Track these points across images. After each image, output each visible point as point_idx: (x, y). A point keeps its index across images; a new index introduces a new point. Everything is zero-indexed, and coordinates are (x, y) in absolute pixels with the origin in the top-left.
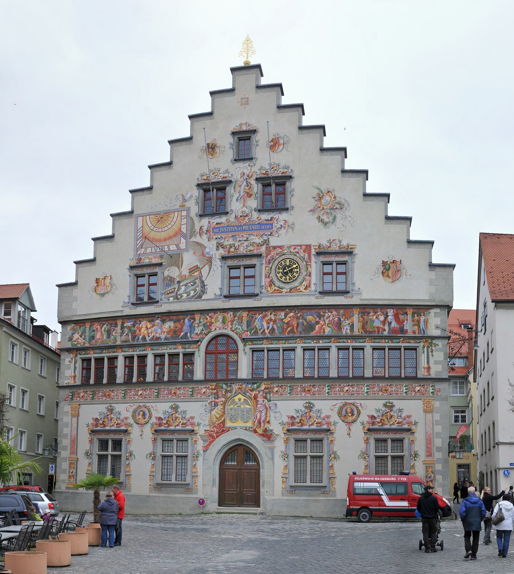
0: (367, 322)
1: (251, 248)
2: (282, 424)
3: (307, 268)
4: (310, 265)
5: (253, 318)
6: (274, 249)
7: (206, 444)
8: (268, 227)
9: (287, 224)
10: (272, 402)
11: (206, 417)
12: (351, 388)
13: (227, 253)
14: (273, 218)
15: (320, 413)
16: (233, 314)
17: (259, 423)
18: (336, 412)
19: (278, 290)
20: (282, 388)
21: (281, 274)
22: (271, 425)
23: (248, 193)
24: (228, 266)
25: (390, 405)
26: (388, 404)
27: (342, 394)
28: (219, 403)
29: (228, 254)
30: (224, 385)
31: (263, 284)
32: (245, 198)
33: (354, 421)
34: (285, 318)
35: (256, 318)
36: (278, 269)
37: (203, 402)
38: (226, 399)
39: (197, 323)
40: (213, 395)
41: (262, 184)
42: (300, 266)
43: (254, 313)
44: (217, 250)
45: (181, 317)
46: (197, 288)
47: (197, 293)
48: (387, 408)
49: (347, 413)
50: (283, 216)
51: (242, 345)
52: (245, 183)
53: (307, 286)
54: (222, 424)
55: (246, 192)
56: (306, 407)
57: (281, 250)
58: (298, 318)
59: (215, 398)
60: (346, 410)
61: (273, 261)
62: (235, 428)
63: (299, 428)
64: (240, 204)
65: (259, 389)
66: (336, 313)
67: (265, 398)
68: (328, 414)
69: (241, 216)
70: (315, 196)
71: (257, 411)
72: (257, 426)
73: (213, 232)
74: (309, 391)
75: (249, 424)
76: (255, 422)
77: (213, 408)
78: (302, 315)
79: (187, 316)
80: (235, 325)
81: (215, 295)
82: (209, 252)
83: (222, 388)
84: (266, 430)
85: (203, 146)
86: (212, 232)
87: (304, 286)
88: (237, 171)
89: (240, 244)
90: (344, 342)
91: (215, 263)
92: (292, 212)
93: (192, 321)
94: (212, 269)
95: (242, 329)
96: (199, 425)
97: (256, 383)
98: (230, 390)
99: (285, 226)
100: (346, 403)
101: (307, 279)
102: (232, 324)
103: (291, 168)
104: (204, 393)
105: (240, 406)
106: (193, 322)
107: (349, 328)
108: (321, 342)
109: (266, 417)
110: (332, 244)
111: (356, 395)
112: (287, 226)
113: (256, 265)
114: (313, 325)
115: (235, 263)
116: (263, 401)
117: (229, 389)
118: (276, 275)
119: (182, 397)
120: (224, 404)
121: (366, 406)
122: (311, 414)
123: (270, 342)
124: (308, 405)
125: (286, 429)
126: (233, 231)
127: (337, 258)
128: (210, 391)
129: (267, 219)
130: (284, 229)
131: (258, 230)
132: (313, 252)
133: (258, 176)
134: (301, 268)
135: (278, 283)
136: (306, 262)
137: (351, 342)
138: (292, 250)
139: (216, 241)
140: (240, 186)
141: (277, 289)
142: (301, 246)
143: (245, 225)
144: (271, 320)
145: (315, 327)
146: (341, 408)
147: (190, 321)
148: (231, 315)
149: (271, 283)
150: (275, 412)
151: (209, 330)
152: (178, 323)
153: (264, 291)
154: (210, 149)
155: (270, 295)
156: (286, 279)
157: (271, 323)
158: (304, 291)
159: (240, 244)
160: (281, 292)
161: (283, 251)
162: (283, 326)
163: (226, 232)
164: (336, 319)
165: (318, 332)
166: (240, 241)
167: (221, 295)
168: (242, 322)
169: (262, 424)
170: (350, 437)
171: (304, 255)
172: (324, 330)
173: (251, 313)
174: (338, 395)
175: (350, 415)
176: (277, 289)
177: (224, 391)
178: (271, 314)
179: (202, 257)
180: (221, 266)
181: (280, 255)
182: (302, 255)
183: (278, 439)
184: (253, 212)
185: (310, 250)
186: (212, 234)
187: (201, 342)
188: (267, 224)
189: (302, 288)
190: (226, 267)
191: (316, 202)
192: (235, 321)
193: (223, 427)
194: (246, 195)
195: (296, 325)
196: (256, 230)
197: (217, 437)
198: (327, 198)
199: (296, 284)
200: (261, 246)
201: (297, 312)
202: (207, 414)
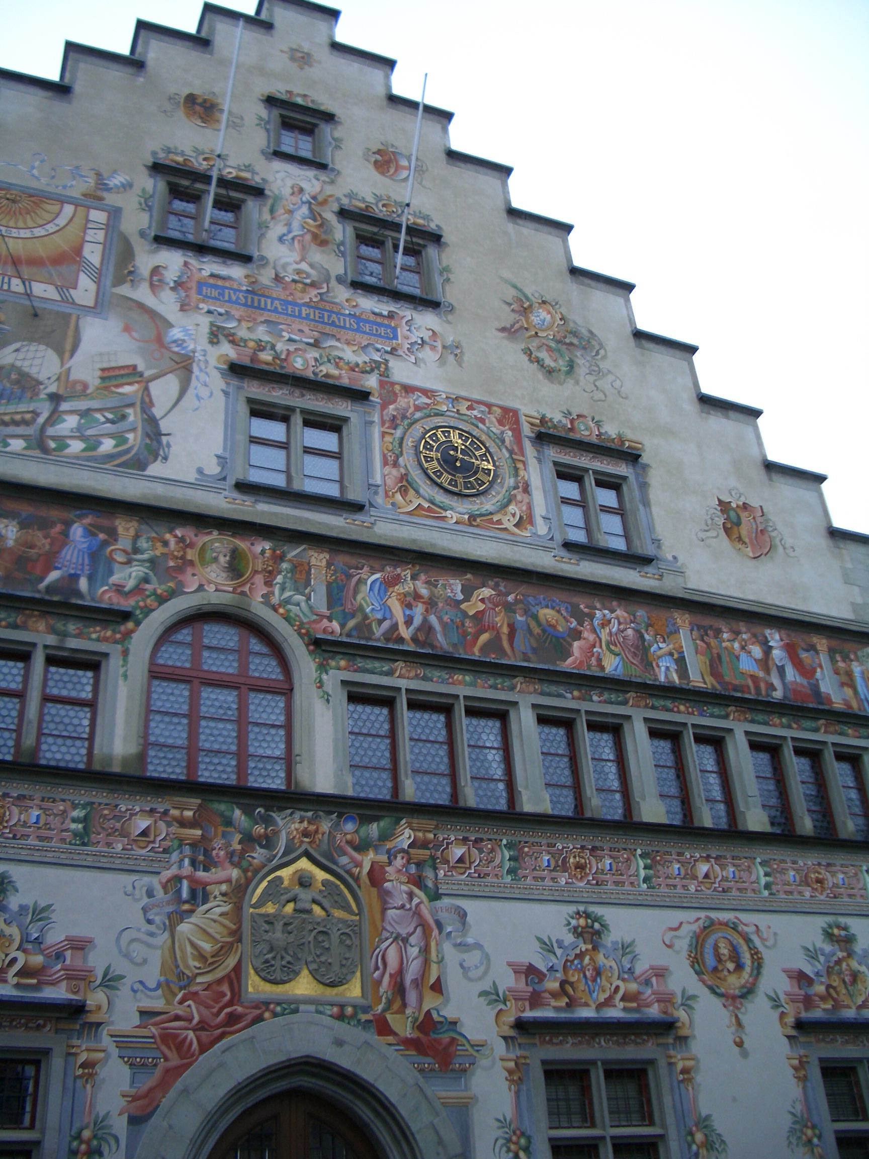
0: (719, 657)
2: (493, 996)
3: (516, 469)
4: (524, 463)
5: (350, 577)
7: (149, 1081)
8: (382, 331)
9: (438, 340)
10: (446, 901)
11: (149, 945)
12: (717, 868)
14: (396, 316)
15: (629, 956)
16: (273, 550)
17: (399, 989)
18: (685, 954)
19: (429, 509)
20: (481, 851)
22: (447, 1000)
23: (315, 237)
24: (250, 401)
25: (843, 933)
26: (836, 931)
27: (692, 888)
28: (216, 890)
30: (237, 813)
31: (378, 480)
33: (748, 992)
34: (467, 599)
35: (361, 581)
37: (134, 877)
38: (245, 871)
39: (125, 551)
40: (187, 850)
41: (355, 228)
43: (352, 560)
45: (55, 513)
46: (130, 436)
47: (127, 451)
48: (837, 946)
49: (719, 958)
50: (427, 320)
51: (313, 666)
52: (305, 210)
53: (521, 517)
54: (225, 988)
56: (578, 932)
57: (428, 401)
58: (509, 608)
59: (193, 863)
60: (716, 948)
61: (406, 422)
62: (292, 1007)
63: (563, 1015)
64: (291, 250)
65: (389, 845)
66: (626, 615)
67: (418, 881)
68: (660, 962)
69: (294, 281)
70: (510, 300)
71: (385, 934)
72: (389, 1003)
73: (199, 292)
74: (580, 867)
75: (354, 990)
76: (379, 982)
77: (186, 907)
78: (521, 601)
79: (80, 517)
80: (283, 589)
81: (200, 471)
82: (184, 341)
83: (229, 822)
84: (427, 1024)
87: (514, 515)
89: (292, 349)
90: (668, 710)
91: (203, 377)
93: (102, 536)
95: (311, 607)
96: (110, 981)
97: (377, 819)
98: (266, 836)
99: (435, 344)
100: (712, 923)
101: (519, 498)
102: (269, 583)
104: (145, 833)
105: (310, 912)
106: (105, 543)
107: (673, 667)
108: (595, 698)
109: (426, 963)
110: (576, 423)
111: (734, 893)
112: (439, 345)
114: (563, 638)
115: (278, 395)
116: (411, 895)
117: (259, 829)
119: (32, 841)
120: (239, 892)
121: (775, 934)
122: (601, 959)
123: (421, 672)
124: (582, 922)
125: (511, 1019)
127: (599, 464)
128: (173, 829)
129: (377, 310)
130: (431, 349)
131: (350, 329)
132: (526, 430)
135: (427, 489)
136: (511, 452)
137: (688, 713)
138: (463, 410)
139: (209, 319)
140: (291, 212)
141: (426, 505)
142: (489, 406)
144: (417, 596)
145: (571, 645)
146: (698, 942)
147: (94, 535)
148: (263, 552)
149: (405, 485)
150: (462, 946)
151: (171, 584)
152: (39, 534)
153: (380, 500)
155: (402, 517)
157: (419, 610)
158: (516, 530)
162: (463, 625)
164: (630, 632)
165: (581, 663)
166: (290, 340)
168: (308, 583)
169: (412, 996)
170: (745, 1054)
172: (599, 660)
173: (342, 560)
174: (679, 890)
175: (731, 966)
176: (426, 505)
177: (238, 837)
178: (414, 578)
180: (226, 393)
181: (425, 411)
183: (484, 1062)
184: (333, 283)
185: (517, 422)
186: (194, 296)
187: (138, 623)
188: (380, 325)
189: (509, 523)
191: (516, 316)
192: (280, 573)
193: (230, 1003)
194: (308, 237)
195: (505, 630)
197: (204, 1048)
198: (541, 316)
199: (488, 504)
200: (362, 372)
201: (502, 588)
202: (152, 934)
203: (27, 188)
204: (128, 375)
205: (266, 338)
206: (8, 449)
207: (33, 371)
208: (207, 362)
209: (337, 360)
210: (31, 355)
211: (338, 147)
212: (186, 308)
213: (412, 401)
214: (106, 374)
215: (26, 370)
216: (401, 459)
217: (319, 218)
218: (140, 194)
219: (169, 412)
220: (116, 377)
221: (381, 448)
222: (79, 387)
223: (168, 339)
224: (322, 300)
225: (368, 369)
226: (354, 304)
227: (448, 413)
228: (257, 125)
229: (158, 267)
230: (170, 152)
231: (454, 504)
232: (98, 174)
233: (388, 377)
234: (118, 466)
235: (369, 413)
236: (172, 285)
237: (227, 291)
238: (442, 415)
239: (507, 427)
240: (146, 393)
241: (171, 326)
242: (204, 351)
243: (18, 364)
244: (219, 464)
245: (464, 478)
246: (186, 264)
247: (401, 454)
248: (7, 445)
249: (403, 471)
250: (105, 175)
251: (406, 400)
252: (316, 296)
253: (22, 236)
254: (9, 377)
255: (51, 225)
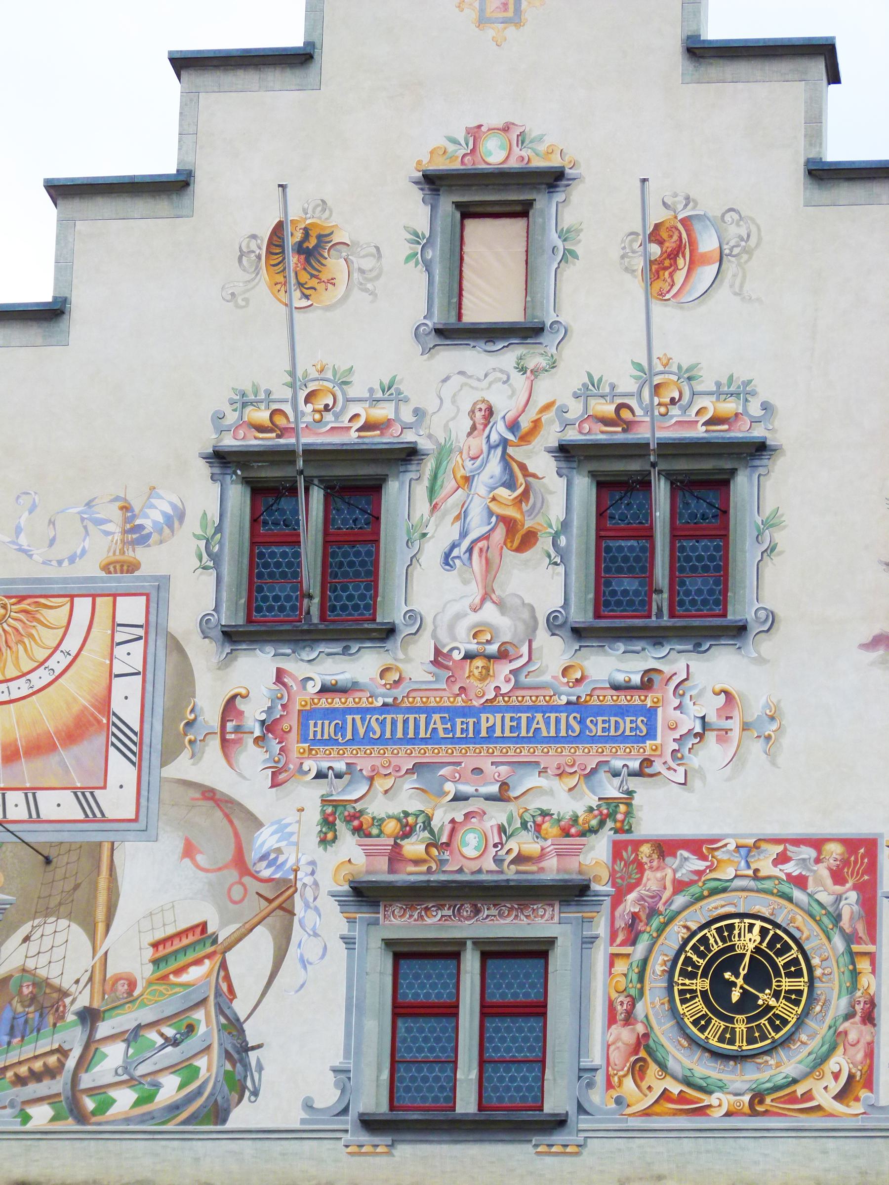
1: (526, 843)
3: (855, 974)
6: (662, 855)
8: (626, 724)
9: (736, 714)
13: (383, 863)
14: (656, 678)
19: (682, 1098)
21: (698, 1004)
23: (510, 524)
29: (391, 871)
31: (596, 1058)
32: (493, 554)
36: (684, 973)
41: (593, 474)
42: (815, 961)
44: (323, 841)
46: (202, 1063)
47: (199, 1092)
52: (494, 467)
53: (851, 1077)
55: (503, 519)
57: (701, 865)
61: (656, 922)
64: (465, 582)
69: (469, 656)
73: (304, 738)
81: (308, 1106)
82: (279, 851)
85: (254, 237)
86: (294, 736)
87: (836, 1076)
88: (447, 391)
89: (459, 818)
92: (767, 646)
94: (293, 952)
99: (728, 724)
101: (852, 1036)
103: (764, 394)
112: (735, 725)
113: (551, 942)
118: (673, 1010)
126: (425, 741)
129: (620, 678)
130: (720, 740)
131: (568, 739)
133: (572, 436)
134: (818, 972)
136: (850, 938)
138: (766, 867)
139: (321, 788)
140: (468, 480)
142: (817, 844)
143: (489, 707)
153: (597, 1097)
154: (293, 260)
156: (728, 1036)
158: (838, 1107)
159: (459, 818)
160: (702, 1111)
161: (711, 869)
163: (381, 740)
166: (458, 798)
167: (345, 1111)
171: (839, 898)
176: (675, 1088)
179: (233, 875)
180: (348, 941)
181: (694, 889)
182: (823, 897)
184: (542, 635)
186: (296, 747)
188: (622, 711)
190: (376, 944)
194: (500, 533)
196: (556, 739)
200: (582, 834)
203: (13, 581)
204: (193, 945)
205: (414, 806)
206: (29, 1127)
207: (52, 973)
208: (316, 883)
209: (539, 819)
210: (47, 942)
211: (569, 255)
212: (282, 777)
213: (669, 872)
214: (162, 952)
215: (42, 973)
216: (639, 1006)
217: (521, 479)
218: (199, 532)
219: (263, 994)
220: (175, 953)
221: (606, 986)
222: (122, 988)
223: (252, 856)
224: (517, 687)
225: (594, 823)
226: (578, 675)
227: (739, 883)
228: (408, 259)
229: (234, 697)
230: (244, 405)
231: (725, 1077)
232: (126, 508)
233: (629, 831)
234: (185, 1122)
235: (591, 920)
236: (257, 733)
237: (349, 718)
238: (724, 890)
239: (848, 885)
240: (222, 974)
241: (259, 825)
242: (313, 863)
243: (31, 964)
244: (336, 1085)
245: (750, 1020)
246: (280, 674)
247: (641, 992)
248: (26, 1118)
249: (640, 1029)
250: (137, 506)
251: (659, 875)
252: (508, 681)
253: (15, 695)
254: (20, 992)
255: (58, 655)
